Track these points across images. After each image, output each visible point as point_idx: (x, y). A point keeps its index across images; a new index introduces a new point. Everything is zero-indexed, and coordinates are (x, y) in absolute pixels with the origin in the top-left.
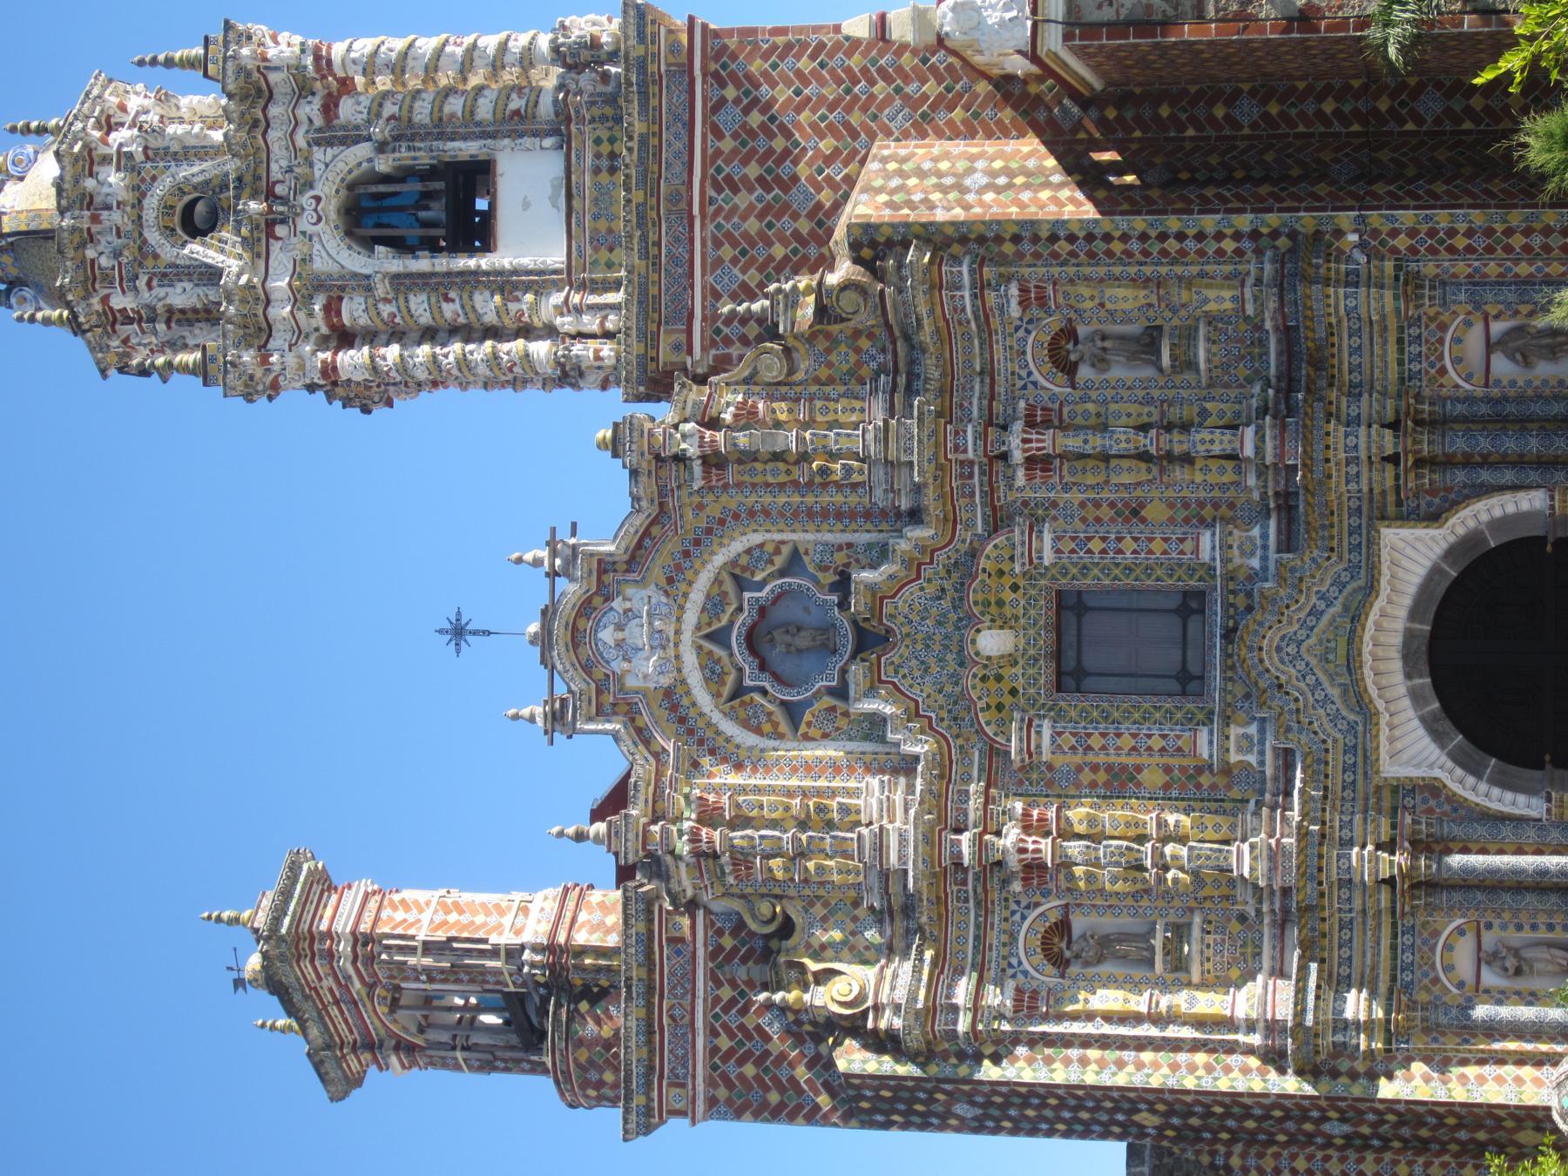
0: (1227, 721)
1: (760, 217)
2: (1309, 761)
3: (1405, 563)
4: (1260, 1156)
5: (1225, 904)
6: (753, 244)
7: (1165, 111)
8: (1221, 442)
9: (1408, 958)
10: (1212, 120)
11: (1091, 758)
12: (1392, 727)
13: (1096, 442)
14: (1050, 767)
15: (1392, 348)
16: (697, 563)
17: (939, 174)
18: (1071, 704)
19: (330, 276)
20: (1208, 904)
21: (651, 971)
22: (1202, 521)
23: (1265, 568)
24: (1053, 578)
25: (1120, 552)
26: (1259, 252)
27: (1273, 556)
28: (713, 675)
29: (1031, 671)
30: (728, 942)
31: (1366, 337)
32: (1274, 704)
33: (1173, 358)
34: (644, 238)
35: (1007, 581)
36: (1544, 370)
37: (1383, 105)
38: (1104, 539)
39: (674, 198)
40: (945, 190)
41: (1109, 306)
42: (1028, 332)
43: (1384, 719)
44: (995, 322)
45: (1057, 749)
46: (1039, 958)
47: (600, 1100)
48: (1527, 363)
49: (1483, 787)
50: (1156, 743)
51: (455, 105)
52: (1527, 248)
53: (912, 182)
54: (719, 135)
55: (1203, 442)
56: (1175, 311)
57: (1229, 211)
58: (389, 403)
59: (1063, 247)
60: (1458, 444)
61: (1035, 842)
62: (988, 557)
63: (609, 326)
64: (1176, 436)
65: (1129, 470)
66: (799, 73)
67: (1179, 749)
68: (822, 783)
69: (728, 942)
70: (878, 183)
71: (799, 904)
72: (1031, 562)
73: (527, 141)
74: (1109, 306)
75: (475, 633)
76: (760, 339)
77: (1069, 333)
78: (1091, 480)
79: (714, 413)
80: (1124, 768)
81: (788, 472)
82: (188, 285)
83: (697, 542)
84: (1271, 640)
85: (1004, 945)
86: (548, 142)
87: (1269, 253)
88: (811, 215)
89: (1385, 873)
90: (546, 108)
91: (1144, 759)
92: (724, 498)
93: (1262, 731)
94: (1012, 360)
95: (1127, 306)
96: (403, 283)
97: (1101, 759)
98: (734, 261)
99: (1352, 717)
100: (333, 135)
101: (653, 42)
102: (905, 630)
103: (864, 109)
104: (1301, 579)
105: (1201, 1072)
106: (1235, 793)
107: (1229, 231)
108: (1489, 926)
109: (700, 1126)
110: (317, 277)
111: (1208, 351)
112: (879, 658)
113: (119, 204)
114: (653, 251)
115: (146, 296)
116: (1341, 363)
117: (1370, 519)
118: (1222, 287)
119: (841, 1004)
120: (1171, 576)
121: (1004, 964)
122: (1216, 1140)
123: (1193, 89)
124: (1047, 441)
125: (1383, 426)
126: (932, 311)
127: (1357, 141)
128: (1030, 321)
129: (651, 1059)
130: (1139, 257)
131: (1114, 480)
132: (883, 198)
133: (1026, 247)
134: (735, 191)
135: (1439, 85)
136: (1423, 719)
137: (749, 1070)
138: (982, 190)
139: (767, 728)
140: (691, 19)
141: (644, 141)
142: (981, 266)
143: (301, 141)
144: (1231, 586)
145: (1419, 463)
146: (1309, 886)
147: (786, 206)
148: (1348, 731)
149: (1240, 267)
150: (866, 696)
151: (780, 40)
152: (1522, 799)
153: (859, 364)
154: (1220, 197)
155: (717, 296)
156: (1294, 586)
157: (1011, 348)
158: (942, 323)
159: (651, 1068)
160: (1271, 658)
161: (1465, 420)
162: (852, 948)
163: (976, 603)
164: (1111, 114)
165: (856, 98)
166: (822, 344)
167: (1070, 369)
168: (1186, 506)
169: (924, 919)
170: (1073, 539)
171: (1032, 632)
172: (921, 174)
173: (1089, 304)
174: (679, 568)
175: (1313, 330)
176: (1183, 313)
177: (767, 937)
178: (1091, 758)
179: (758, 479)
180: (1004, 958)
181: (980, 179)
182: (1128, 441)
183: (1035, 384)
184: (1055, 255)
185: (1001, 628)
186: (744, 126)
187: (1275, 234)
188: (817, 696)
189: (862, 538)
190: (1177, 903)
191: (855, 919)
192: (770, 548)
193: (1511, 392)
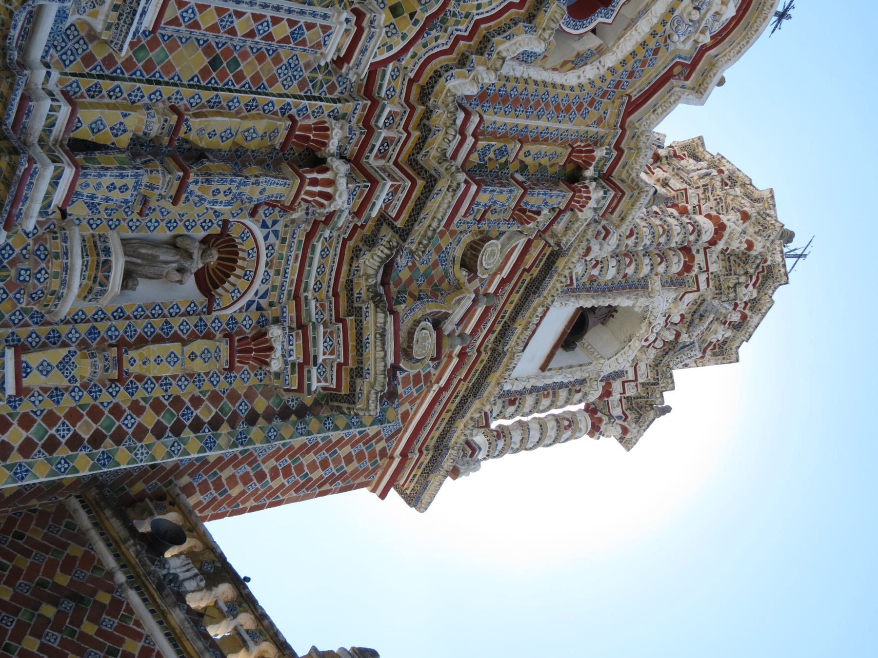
33: (106, 266)
38: (269, 37)
55: (124, 188)
59: (206, 413)
62: (403, 38)
72: (359, 15)
94: (281, 257)
96: (640, 286)
101: (415, 476)
111: (64, 283)
113: (725, 323)
114: (498, 328)
140: (383, 496)
151: (327, 487)
157: (277, 273)
182: (217, 192)
183: (264, 225)
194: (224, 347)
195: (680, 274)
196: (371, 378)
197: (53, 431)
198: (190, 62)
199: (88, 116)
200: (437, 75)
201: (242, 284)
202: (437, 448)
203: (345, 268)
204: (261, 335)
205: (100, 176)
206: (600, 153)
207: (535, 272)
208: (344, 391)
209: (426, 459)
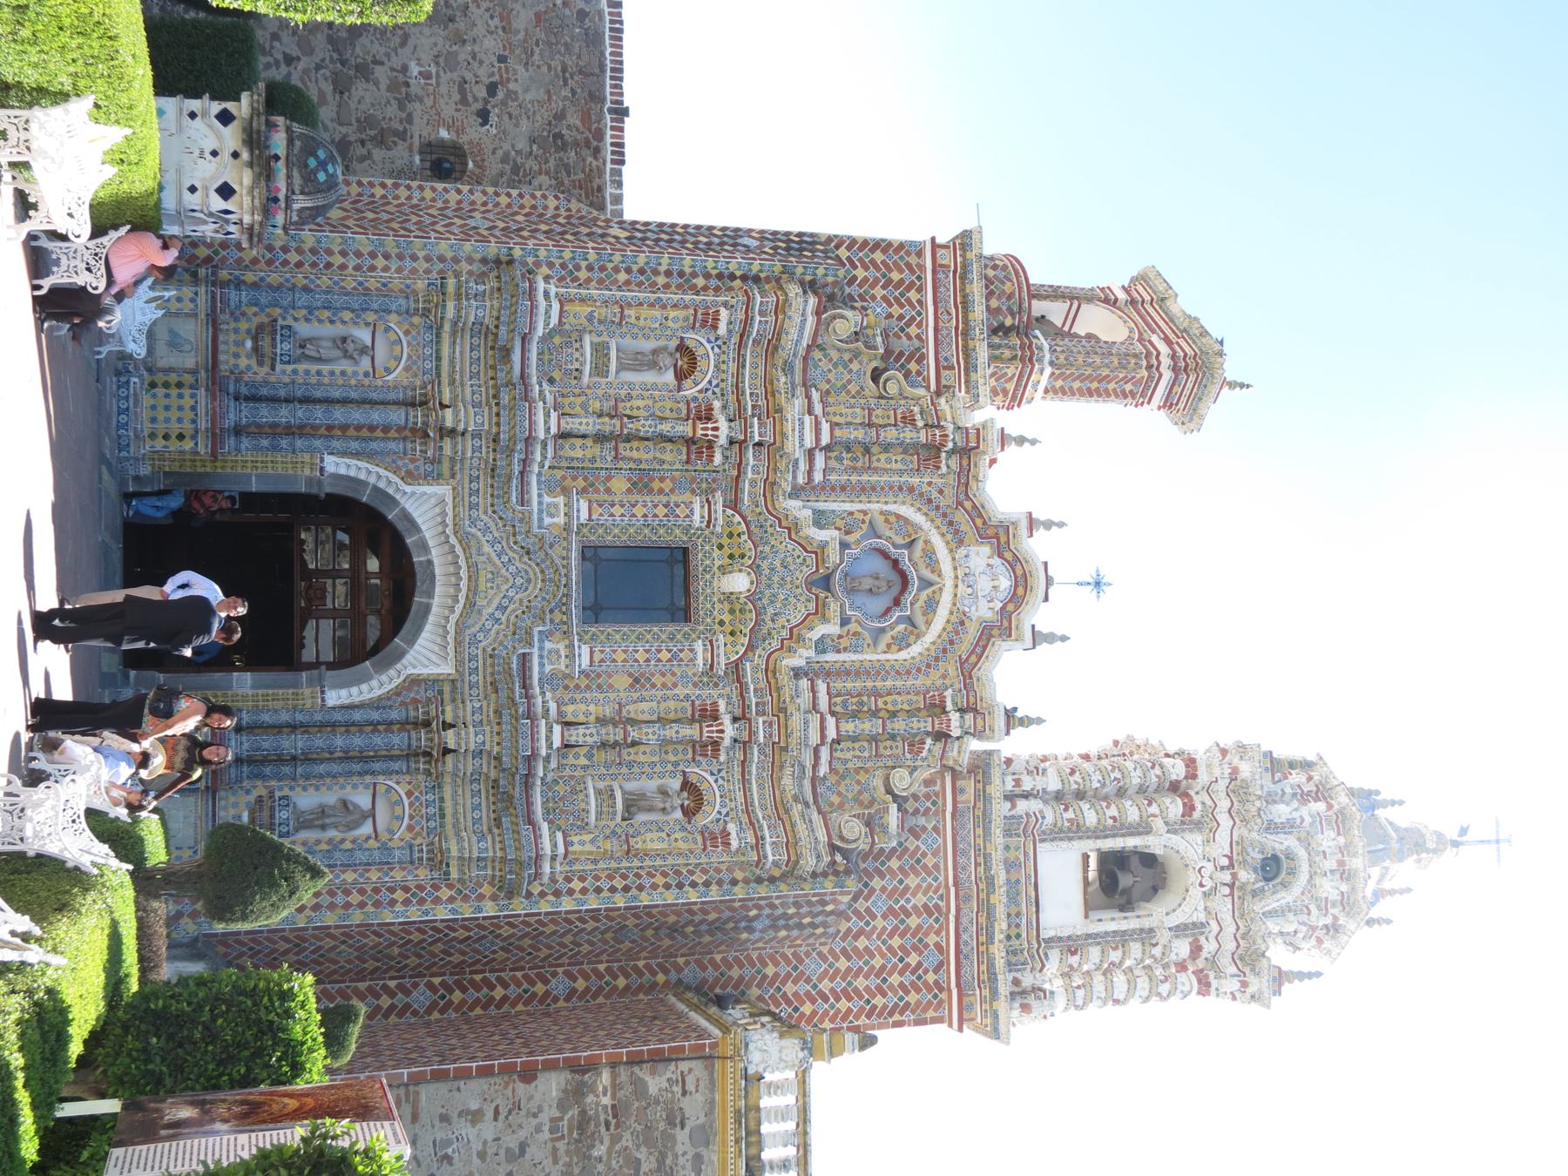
0: (567, 528)
1: (907, 888)
3: (436, 649)
4: (534, 207)
5: (565, 391)
6: (912, 867)
7: (621, 982)
8: (576, 735)
9: (428, 351)
10: (586, 977)
11: (664, 499)
12: (443, 523)
13: (670, 732)
14: (693, 492)
15: (449, 811)
17: (787, 927)
18: (678, 537)
19: (1191, 831)
20: (577, 391)
21: (965, 347)
22: (587, 676)
23: (541, 641)
24: (694, 631)
25: (647, 651)
26: (553, 880)
27: (535, 651)
28: (930, 554)
30: (913, 366)
31: (469, 819)
32: (533, 539)
33: (612, 796)
34: (988, 868)
35: (728, 628)
36: (330, 798)
37: (457, 996)
38: (659, 660)
39: (968, 898)
40: (785, 916)
41: (664, 835)
44: (745, 819)
45: (689, 504)
46: (700, 352)
47: (992, 258)
48: (345, 803)
49: (372, 480)
50: (617, 510)
51: (1115, 956)
52: (347, 892)
53: (807, 920)
54: (937, 945)
55: (591, 735)
56: (613, 832)
57: (579, 911)
58: (1116, 743)
59: (699, 878)
60: (398, 740)
63: (1008, 805)
64: (612, 739)
65: (643, 712)
66: (884, 995)
68: (854, 478)
69: (913, 366)
70: (830, 919)
71: (867, 392)
73: (1066, 933)
74: (664, 835)
76: (905, 799)
77: (689, 813)
78: (672, 704)
79: (939, 745)
80: (640, 491)
81: (886, 703)
82: (1277, 820)
83: (945, 651)
86: (1052, 933)
87: (546, 879)
88: (872, 891)
89: (449, 413)
90: (1054, 955)
92: (929, 682)
93: (540, 520)
95: (649, 836)
96: (1143, 828)
97: (657, 499)
98: (924, 855)
99: (473, 530)
100: (1191, 930)
103: (838, 971)
105: (584, 264)
106: (559, 474)
108: (366, 374)
109: (928, 238)
110: (1200, 830)
115: (1304, 811)
118: (582, 853)
119: (842, 317)
121: (724, 348)
122: (568, 217)
123: (601, 1000)
124: (708, 732)
126: (793, 825)
127: (479, 967)
128: (718, 820)
129: (963, 283)
132: (829, 908)
133: (726, 877)
134: (925, 906)
135: (415, 1013)
136: (417, 529)
137: (895, 276)
138: (757, 917)
139: (892, 519)
140: (960, 1029)
141: (990, 939)
142: (759, 861)
143: (1214, 926)
144: (565, 628)
145: (427, 724)
147: (890, 896)
151: (896, 1017)
152: (342, 471)
153: (838, 783)
154: (584, 921)
155: (935, 829)
158: (785, 817)
159: (963, 278)
161: (391, 758)
164: (661, 978)
166: (866, 797)
167: (687, 785)
168: (599, 686)
169: (783, 379)
172: (800, 926)
173: (678, 835)
174: (957, 633)
176: (608, 832)
177: (886, 370)
178: (664, 499)
179: (905, 698)
181: (758, 925)
182: (647, 734)
184: (704, 871)
186: (921, 953)
187: (542, 894)
188: (858, 542)
189: (831, 657)
190: (600, 392)
191: (828, 381)
193: (355, 779)
194: (700, 839)
198: (622, 682)
206: (949, 693)
207: (980, 805)
209: (986, 992)
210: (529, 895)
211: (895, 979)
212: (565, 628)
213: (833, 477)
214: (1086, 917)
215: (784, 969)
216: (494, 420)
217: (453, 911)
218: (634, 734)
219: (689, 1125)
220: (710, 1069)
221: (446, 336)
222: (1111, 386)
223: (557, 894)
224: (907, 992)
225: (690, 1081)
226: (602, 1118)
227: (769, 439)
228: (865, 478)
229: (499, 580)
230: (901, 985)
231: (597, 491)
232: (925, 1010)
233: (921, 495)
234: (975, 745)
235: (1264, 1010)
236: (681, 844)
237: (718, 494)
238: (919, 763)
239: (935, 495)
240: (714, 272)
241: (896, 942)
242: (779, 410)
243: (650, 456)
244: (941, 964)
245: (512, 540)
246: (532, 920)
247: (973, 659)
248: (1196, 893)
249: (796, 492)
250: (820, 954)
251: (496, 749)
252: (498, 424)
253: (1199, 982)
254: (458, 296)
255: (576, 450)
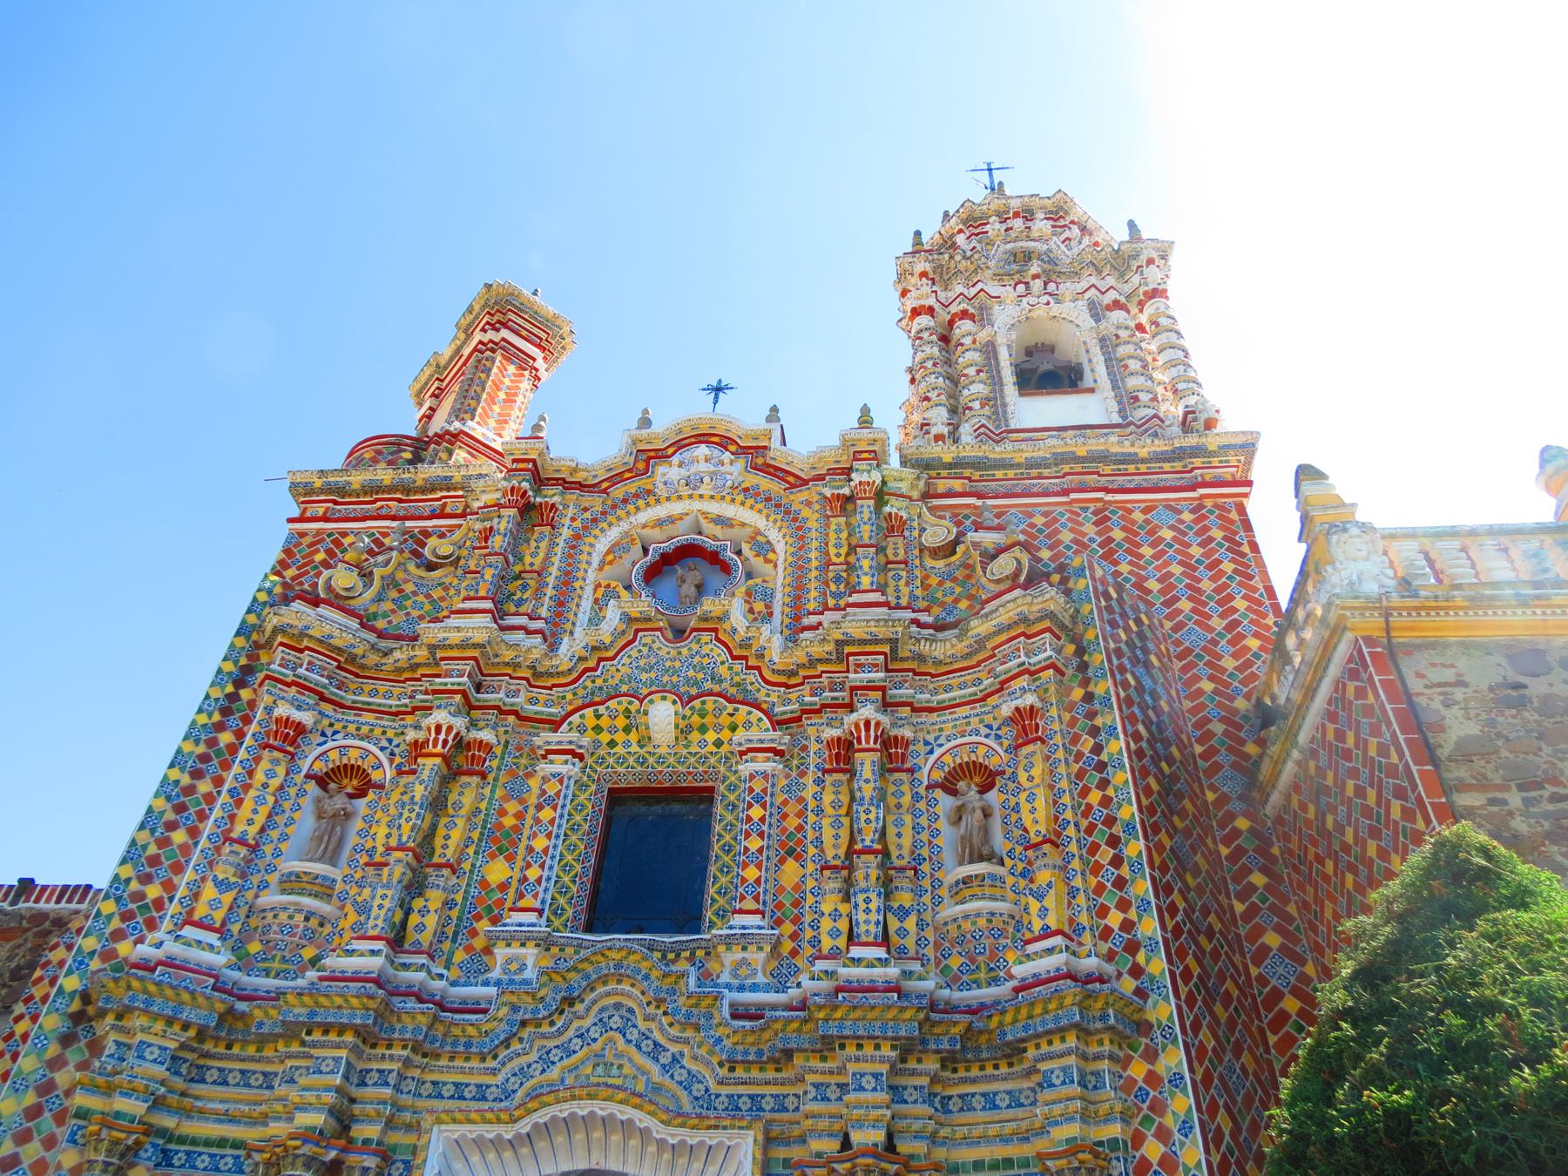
0: (546, 943)
1: (1075, 541)
2: (471, 1031)
7: (1258, 879)
10: (1258, 931)
12: (497, 1143)
13: (868, 791)
14: (529, 775)
15: (1000, 1152)
16: (760, 506)
18: (590, 803)
24: (725, 778)
26: (1110, 957)
29: (631, 760)
33: (966, 881)
35: (725, 735)
38: (762, 819)
42: (987, 736)
43: (508, 1132)
50: (533, 874)
54: (1146, 511)
55: (867, 901)
61: (445, 742)
62: (749, 713)
65: (837, 837)
67: (522, 896)
68: (550, 592)
71: (447, 581)
72: (742, 754)
74: (1023, 796)
75: (716, 398)
80: (515, 844)
81: (838, 555)
84: (629, 995)
85: (358, 729)
91: (519, 863)
95: (1027, 820)
96: (990, 350)
97: (529, 821)
98: (1032, 525)
100: (1096, 311)
102: (685, 651)
103: (1194, 610)
104: (697, 1028)
107: (1132, 915)
111: (978, 915)
112: (660, 629)
114: (1034, 472)
116: (974, 1081)
117: (769, 1122)
120: (719, 893)
121: (338, 726)
123: (1291, 909)
125: (890, 1136)
128: (998, 737)
130: (1084, 823)
131: (826, 822)
134: (1096, 524)
139: (610, 557)
142: (1053, 666)
144: (700, 953)
146: (302, 1011)
148: (504, 1091)
149: (1087, 934)
150: (623, 613)
151: (1246, 549)
153: (942, 604)
156: (689, 1015)
157: (968, 724)
160: (608, 994)
162: (393, 611)
163: (704, 703)
165: (1205, 604)
168: (796, 904)
170: (764, 791)
171: (672, 760)
173: (1022, 776)
175: (1015, 1021)
176: (1022, 883)
178: (531, 811)
179: (833, 536)
180: (345, 727)
182: (868, 821)
183: (931, 752)
184: (1075, 739)
185: (677, 726)
187: (1136, 971)
192: (771, 556)
195: (972, 318)
196: (1025, 609)
197: (1109, 885)
199: (827, 944)
200: (779, 672)
201: (982, 750)
202: (1180, 459)
203: (956, 666)
204: (1011, 720)
205: (858, 924)
207: (967, 473)
208: (1047, 624)
209: (1198, 462)
210: (1140, 993)
211: (1196, 551)
212: (700, 953)
213: (544, 612)
214: (1092, 390)
215: (1201, 669)
216: (333, 1037)
217: (1186, 1128)
218: (868, 839)
219: (1514, 677)
220: (1411, 649)
221: (193, 1128)
222: (507, 381)
223: (1132, 947)
224: (1211, 539)
225: (1436, 675)
226: (1551, 807)
227: (468, 667)
228: (551, 580)
229: (609, 1057)
230: (1202, 545)
231: (501, 902)
232: (1232, 522)
233: (585, 528)
234: (894, 461)
235: (1176, 247)
236: (1036, 772)
237: (537, 741)
238: (915, 524)
239: (587, 515)
240: (217, 717)
241: (1147, 551)
242: (433, 648)
243: (460, 822)
244: (1168, 507)
245: (545, 1029)
246: (1183, 990)
247: (791, 479)
248: (1055, 309)
249: (553, 648)
250: (1176, 629)
251: (887, 1051)
252: (342, 1029)
253: (1151, 298)
254: (108, 1091)
255: (427, 921)
